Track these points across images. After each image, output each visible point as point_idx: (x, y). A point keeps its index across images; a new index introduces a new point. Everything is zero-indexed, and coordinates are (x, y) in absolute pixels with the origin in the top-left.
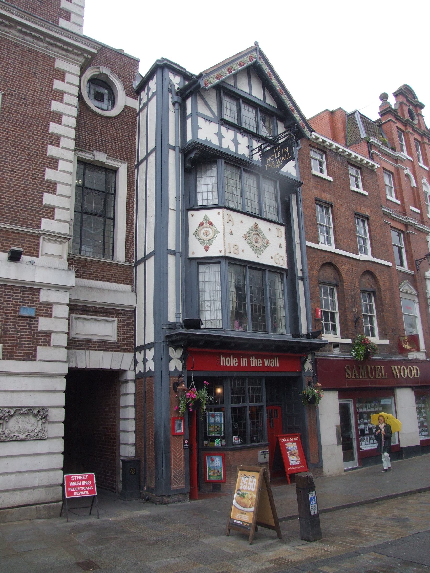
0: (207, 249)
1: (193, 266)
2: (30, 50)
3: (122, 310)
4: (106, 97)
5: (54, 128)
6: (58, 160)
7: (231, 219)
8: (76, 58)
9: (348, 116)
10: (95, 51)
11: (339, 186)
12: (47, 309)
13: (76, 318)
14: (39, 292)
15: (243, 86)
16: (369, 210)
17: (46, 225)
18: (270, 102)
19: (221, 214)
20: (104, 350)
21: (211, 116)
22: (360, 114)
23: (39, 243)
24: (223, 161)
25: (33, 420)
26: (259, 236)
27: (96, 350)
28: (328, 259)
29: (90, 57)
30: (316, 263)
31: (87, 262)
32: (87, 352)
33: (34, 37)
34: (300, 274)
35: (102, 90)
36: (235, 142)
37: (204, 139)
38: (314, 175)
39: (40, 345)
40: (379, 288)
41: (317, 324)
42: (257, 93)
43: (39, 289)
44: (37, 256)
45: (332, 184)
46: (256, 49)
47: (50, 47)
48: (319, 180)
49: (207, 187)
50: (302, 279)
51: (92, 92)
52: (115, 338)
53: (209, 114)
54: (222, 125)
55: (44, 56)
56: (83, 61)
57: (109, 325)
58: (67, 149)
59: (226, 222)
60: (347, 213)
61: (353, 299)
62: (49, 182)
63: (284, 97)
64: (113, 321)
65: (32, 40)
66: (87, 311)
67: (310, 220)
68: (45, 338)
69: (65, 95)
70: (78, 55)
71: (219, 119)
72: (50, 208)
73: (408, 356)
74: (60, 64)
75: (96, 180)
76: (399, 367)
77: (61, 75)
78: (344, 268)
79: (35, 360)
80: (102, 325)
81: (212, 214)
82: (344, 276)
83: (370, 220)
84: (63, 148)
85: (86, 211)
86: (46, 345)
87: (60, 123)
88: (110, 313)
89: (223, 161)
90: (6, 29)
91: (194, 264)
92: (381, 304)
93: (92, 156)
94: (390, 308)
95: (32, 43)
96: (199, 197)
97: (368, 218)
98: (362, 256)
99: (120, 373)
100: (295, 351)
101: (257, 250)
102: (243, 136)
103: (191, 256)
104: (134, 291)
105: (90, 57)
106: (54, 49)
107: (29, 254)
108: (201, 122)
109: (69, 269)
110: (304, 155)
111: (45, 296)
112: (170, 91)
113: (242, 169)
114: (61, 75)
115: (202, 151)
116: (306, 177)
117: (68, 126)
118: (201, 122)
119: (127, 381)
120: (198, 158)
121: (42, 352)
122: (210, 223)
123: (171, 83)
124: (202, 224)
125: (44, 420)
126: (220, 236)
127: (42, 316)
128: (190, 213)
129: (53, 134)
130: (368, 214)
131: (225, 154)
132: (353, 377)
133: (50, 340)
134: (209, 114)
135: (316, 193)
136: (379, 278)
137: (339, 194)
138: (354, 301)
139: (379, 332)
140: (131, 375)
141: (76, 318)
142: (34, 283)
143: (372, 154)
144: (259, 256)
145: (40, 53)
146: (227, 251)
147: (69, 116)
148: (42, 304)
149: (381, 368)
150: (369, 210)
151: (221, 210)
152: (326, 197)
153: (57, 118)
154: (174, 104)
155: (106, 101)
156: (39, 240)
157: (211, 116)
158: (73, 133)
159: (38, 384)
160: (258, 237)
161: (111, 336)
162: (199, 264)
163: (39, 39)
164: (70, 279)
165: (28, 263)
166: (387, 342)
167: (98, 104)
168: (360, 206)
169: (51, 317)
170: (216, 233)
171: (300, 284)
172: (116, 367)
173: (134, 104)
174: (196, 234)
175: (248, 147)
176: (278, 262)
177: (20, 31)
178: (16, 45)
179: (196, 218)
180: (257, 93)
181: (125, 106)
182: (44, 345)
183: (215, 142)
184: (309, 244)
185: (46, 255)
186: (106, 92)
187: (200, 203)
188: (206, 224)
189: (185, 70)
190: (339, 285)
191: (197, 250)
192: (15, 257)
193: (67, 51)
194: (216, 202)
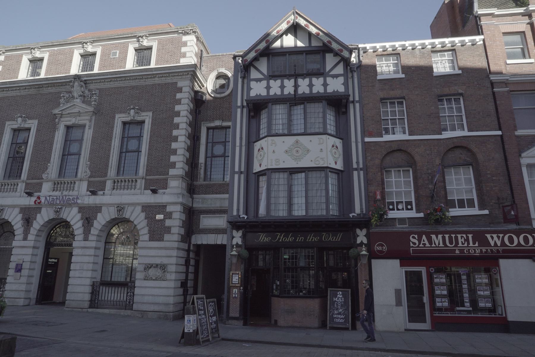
0: (260, 165)
1: (252, 179)
2: (165, 84)
7: (273, 142)
12: (169, 216)
17: (172, 172)
24: (270, 104)
25: (159, 270)
34: (355, 166)
53: (260, 76)
54: (271, 79)
55: (172, 84)
61: (430, 177)
68: (168, 230)
73: (531, 225)
74: (180, 84)
76: (501, 235)
77: (180, 90)
82: (417, 158)
90: (153, 79)
97: (461, 94)
99: (223, 247)
103: (254, 172)
106: (175, 77)
111: (169, 209)
114: (180, 90)
115: (253, 103)
121: (167, 237)
124: (259, 150)
128: (255, 144)
129: (175, 124)
130: (460, 91)
134: (260, 76)
135: (382, 95)
136: (475, 150)
139: (478, 203)
147: (184, 110)
149: (468, 237)
166: (486, 212)
170: (265, 154)
174: (257, 158)
177: (159, 77)
178: (159, 85)
183: (264, 93)
184: (367, 140)
185: (172, 188)
188: (261, 150)
192: (154, 191)
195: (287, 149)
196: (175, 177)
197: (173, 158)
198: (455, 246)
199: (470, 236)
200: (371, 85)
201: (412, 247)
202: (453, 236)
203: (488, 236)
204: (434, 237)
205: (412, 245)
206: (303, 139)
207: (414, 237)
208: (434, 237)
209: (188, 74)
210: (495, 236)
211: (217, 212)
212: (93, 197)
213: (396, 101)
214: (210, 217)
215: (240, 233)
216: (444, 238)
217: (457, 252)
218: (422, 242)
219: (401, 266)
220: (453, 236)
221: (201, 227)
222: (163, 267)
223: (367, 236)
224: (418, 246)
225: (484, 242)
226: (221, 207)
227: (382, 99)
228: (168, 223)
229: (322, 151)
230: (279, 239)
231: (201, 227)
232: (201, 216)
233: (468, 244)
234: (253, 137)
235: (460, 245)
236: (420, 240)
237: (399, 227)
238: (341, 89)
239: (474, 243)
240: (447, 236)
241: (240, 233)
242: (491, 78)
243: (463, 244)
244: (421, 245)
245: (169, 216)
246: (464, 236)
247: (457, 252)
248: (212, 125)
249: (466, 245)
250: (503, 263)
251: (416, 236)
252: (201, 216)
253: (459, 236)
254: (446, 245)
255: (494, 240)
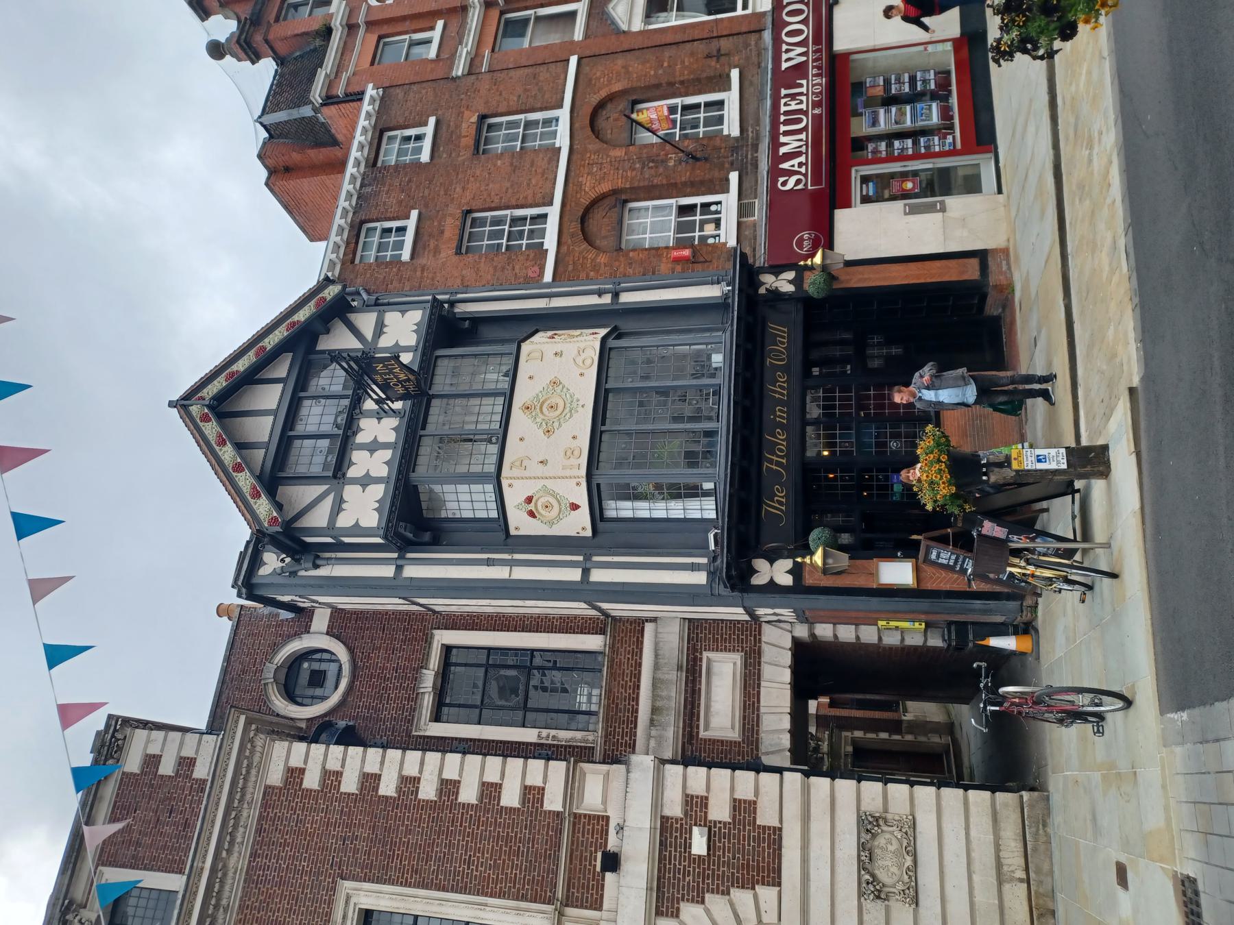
0: (575, 507)
1: (607, 535)
2: (259, 831)
3: (688, 642)
4: (316, 666)
5: (388, 788)
6: (442, 780)
7: (518, 463)
8: (259, 749)
9: (271, 136)
10: (243, 718)
11: (427, 192)
12: (696, 805)
13: (707, 728)
14: (668, 818)
15: (262, 429)
16: (467, 113)
17: (553, 802)
18: (282, 369)
19: (510, 481)
20: (759, 679)
21: (331, 497)
22: (264, 112)
23: (585, 815)
24: (412, 475)
25: (881, 841)
26: (543, 402)
27: (759, 693)
28: (575, 227)
29: (254, 727)
30: (584, 258)
31: (609, 705)
32: (762, 710)
33: (235, 827)
34: (607, 299)
35: (304, 678)
36: (373, 447)
37: (376, 515)
38: (413, 256)
39: (755, 819)
40: (624, 93)
41: (702, 259)
42: (270, 397)
43: (662, 817)
44: (608, 818)
45: (423, 211)
46: (182, 405)
47: (248, 797)
48: (420, 244)
49: (464, 502)
50: (616, 295)
51: (310, 692)
52: (737, 657)
53: (328, 502)
54: (344, 475)
55: (265, 805)
56: (262, 736)
57: (716, 667)
58: (422, 763)
59: (527, 473)
60: (478, 173)
62: (481, 797)
63: (271, 342)
64: (709, 660)
65: (241, 830)
66: (693, 708)
67: (503, 268)
68: (744, 809)
69: (328, 767)
70: (253, 747)
71: (335, 482)
72: (525, 794)
73: (764, 14)
74: (275, 776)
75: (466, 682)
76: (784, 47)
77: (294, 775)
78: (591, 188)
79: (780, 829)
80: (715, 681)
81: (513, 499)
82: (605, 187)
83: (485, 111)
84: (421, 772)
85: (522, 702)
86: (755, 809)
87: (377, 777)
88: (695, 665)
89: (412, 475)
91: (601, 525)
92: (658, 86)
93: (427, 696)
94: (666, 64)
95: (246, 828)
96: (482, 514)
97: (483, 117)
98: (563, 140)
100: (752, 310)
101: (571, 409)
102: (359, 430)
103: (589, 533)
104: (654, 620)
105: (254, 727)
106: (250, 790)
107: (605, 833)
108: (344, 521)
109: (626, 763)
110: (376, 278)
111: (674, 808)
112: (293, 574)
113: (422, 433)
114: (294, 775)
115: (399, 520)
116: (419, 273)
117: (382, 763)
118: (344, 521)
119: (813, 635)
120: (414, 523)
121: (766, 817)
122: (529, 500)
123: (279, 571)
124: (532, 514)
125: (881, 822)
126: (550, 484)
127: (706, 813)
128: (513, 532)
129: (399, 790)
130: (474, 119)
131: (399, 472)
132: (803, 170)
133: (745, 801)
134: (328, 502)
135: (447, 252)
137: (442, 193)
138: (653, 161)
139: (714, 91)
140: (802, 632)
141: (706, 729)
142: (653, 829)
143: (347, 95)
144: (581, 403)
145: (260, 813)
146: (575, 472)
147: (363, 761)
148: (686, 814)
149: (786, 96)
150: (467, 113)
151: (505, 483)
152: (450, 226)
153: (370, 781)
154: (316, 567)
155: (324, 666)
156: (580, 815)
157: (331, 497)
158: (394, 754)
159: (818, 817)
160: (545, 405)
161: (735, 664)
162: (602, 519)
163: (237, 818)
164: (643, 762)
165: (620, 835)
166: (735, 74)
167: (330, 682)
168: (459, 137)
169: (707, 798)
170: (547, 491)
171: (627, 298)
172: (787, 658)
173: (321, 621)
174: (551, 523)
175: (379, 419)
176: (588, 362)
177: (229, 852)
178: (254, 855)
179: (520, 523)
180: (270, 397)
181: (327, 633)
182: (755, 813)
183: (378, 491)
184: (548, 277)
185: (604, 802)
186: (306, 665)
187: (494, 514)
188: (531, 507)
189: (248, 543)
190: (624, 197)
191: (579, 523)
192: (612, 862)
193: (249, 767)
194: (490, 488)
195: (541, 432)
196: (572, 787)
197: (511, 798)
198: (805, 113)
199: (784, 92)
200: (419, 273)
201: (806, 185)
202: (782, 118)
203: (784, 66)
204: (783, 150)
205: (800, 187)
206: (522, 395)
207: (784, 184)
208: (783, 150)
209: (251, 741)
210: (784, 56)
211: (694, 681)
212: (626, 866)
213: (468, 230)
214: (708, 707)
215: (761, 564)
216: (786, 133)
217: (817, 111)
218: (796, 168)
219: (849, 206)
220: (783, 128)
221: (734, 735)
222: (869, 825)
223: (776, 270)
224: (805, 175)
225: (800, 70)
226: (679, 668)
227: (458, 251)
228: (720, 811)
229: (561, 367)
230: (778, 464)
231: (734, 735)
232: (703, 734)
233: (801, 94)
234: (494, 535)
235: (803, 106)
236: (790, 173)
237: (759, 213)
238: (416, 316)
239: (801, 86)
240: (783, 128)
241: (761, 564)
242: (460, 73)
243: (801, 102)
244: (803, 170)
245: (696, 805)
246: (783, 101)
247: (817, 111)
248: (428, 701)
249: (804, 98)
250: (840, 45)
251: (781, 180)
252: (703, 734)
253: (783, 109)
254: (805, 129)
255: (793, 57)
